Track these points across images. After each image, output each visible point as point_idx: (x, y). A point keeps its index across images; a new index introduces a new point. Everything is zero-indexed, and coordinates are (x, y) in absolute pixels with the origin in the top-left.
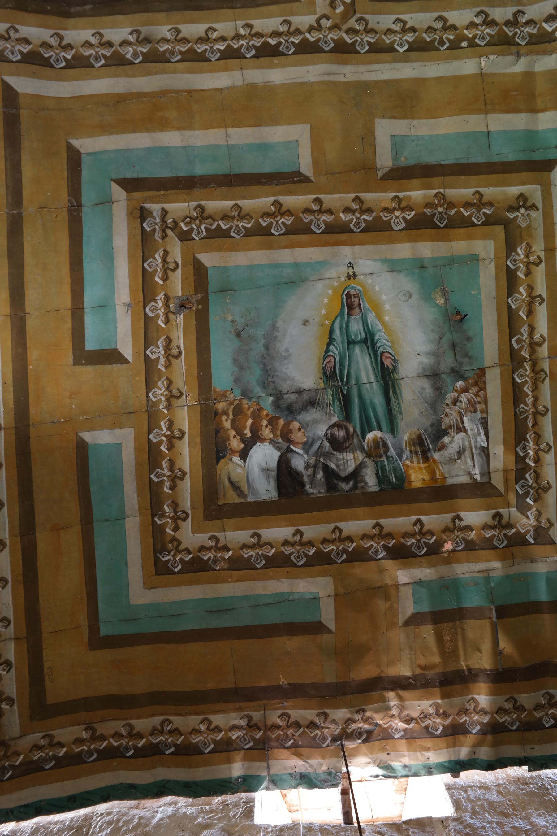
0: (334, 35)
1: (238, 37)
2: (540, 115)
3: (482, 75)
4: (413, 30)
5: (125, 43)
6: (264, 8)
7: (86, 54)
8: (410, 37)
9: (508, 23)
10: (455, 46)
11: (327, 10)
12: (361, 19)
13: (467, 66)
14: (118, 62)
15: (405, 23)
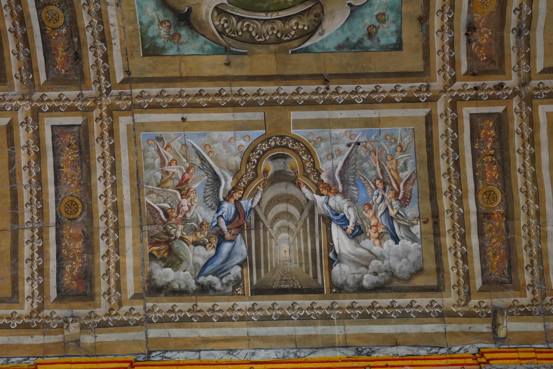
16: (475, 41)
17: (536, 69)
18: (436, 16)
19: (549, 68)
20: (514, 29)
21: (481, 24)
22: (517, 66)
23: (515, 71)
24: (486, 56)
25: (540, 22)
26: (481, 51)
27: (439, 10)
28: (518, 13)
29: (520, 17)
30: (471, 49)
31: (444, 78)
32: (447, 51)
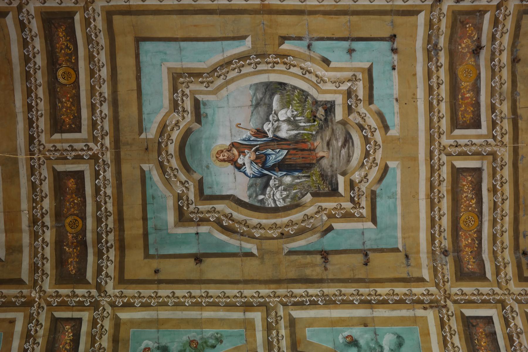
0: (36, 151)
1: (37, 111)
2: (4, 235)
3: (21, 211)
4: (41, 184)
5: (35, 63)
6: (49, 122)
7: (29, 47)
8: (38, 182)
9: (43, 223)
10: (34, 201)
11: (47, 148)
12: (44, 162)
13: (24, 205)
14: (27, 60)
15: (44, 181)
16: (474, 41)
17: (425, 14)
18: (505, 63)
19: (413, 15)
20: (441, 50)
21: (469, 55)
22: (442, 18)
23: (443, 13)
24: (467, 28)
25: (420, 56)
26: (470, 32)
27: (503, 68)
28: (439, 64)
29: (438, 60)
30: (478, 34)
31: (507, 9)
32: (499, 33)
